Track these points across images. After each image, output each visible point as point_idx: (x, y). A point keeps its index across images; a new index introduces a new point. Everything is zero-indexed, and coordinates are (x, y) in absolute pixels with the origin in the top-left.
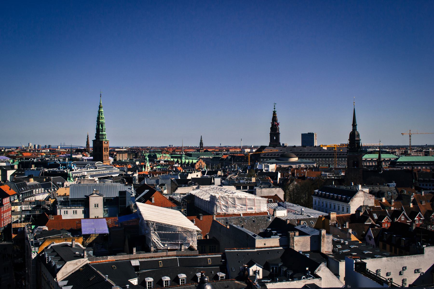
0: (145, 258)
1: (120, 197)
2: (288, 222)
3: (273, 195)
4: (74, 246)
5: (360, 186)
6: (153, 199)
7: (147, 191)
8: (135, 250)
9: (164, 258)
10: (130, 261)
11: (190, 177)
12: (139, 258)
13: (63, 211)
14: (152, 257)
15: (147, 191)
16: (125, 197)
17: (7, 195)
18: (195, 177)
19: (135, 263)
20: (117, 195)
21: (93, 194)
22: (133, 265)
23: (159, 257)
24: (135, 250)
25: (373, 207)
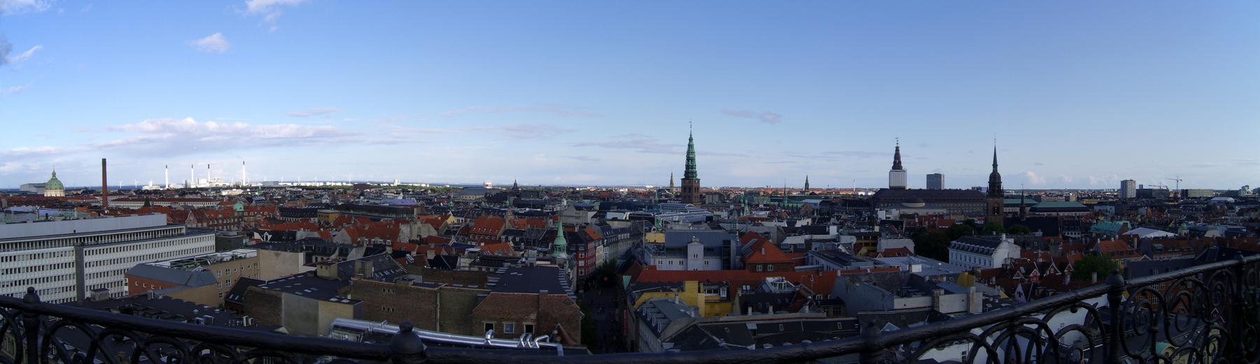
0: (762, 320)
1: (724, 247)
2: (927, 279)
3: (902, 247)
4: (677, 302)
5: (1004, 235)
6: (763, 249)
7: (754, 240)
8: (771, 308)
9: (785, 321)
10: (745, 324)
11: (799, 224)
12: (756, 320)
13: (657, 260)
14: (771, 320)
15: (754, 240)
16: (730, 247)
17: (592, 240)
18: (805, 224)
19: (752, 326)
20: (720, 243)
21: (692, 242)
22: (749, 328)
23: (779, 319)
24: (750, 309)
25: (1018, 260)
